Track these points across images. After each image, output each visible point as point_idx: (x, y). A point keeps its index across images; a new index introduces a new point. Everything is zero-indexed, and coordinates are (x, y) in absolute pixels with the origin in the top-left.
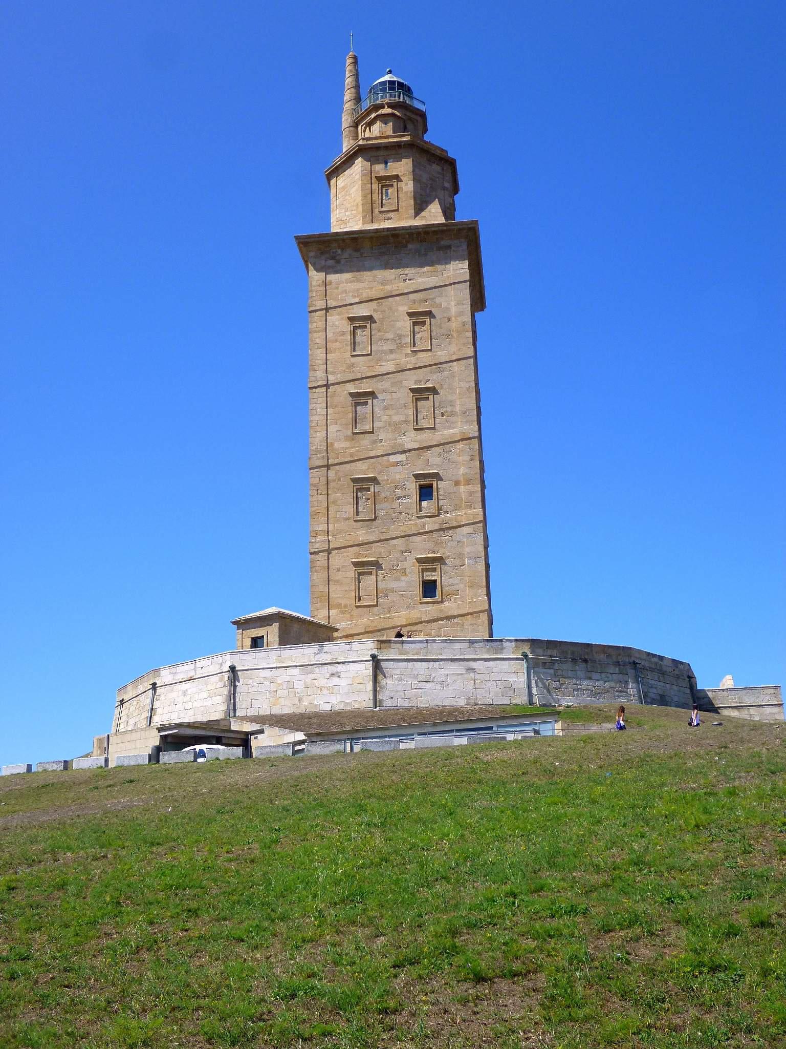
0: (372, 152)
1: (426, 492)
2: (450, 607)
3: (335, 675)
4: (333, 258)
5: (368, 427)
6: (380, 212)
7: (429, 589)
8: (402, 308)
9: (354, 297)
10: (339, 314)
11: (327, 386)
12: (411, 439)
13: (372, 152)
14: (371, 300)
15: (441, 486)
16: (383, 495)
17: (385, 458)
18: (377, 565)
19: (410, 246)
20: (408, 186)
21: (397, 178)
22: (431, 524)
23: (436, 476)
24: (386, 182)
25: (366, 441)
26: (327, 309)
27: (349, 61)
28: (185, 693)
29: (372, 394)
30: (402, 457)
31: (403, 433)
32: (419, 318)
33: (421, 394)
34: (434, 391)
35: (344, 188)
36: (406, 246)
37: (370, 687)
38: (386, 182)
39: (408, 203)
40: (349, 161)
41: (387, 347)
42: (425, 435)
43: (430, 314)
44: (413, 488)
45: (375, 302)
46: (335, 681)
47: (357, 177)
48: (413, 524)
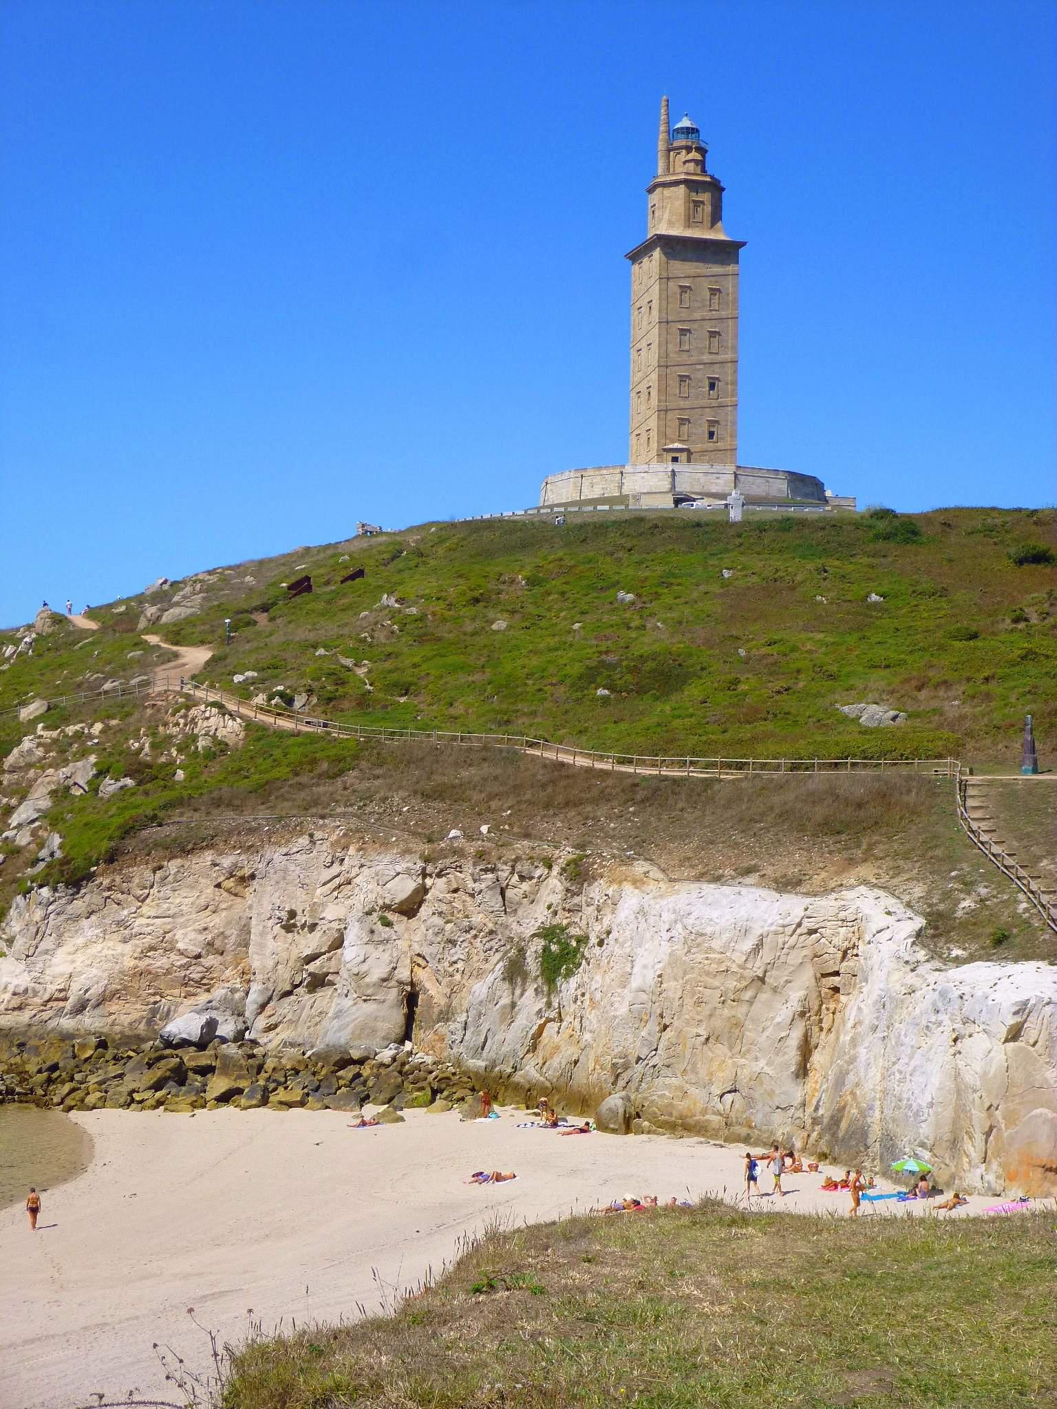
0: (691, 185)
1: (712, 386)
2: (720, 445)
5: (686, 348)
7: (711, 435)
8: (706, 284)
11: (667, 322)
12: (706, 358)
13: (691, 185)
15: (719, 385)
18: (688, 420)
20: (708, 209)
21: (702, 202)
22: (714, 403)
23: (717, 379)
24: (697, 204)
25: (685, 355)
26: (668, 279)
27: (664, 103)
29: (689, 331)
31: (703, 354)
32: (714, 292)
33: (713, 334)
34: (719, 333)
35: (670, 198)
38: (697, 204)
39: (707, 219)
40: (676, 183)
41: (697, 304)
43: (719, 290)
44: (707, 383)
48: (705, 402)
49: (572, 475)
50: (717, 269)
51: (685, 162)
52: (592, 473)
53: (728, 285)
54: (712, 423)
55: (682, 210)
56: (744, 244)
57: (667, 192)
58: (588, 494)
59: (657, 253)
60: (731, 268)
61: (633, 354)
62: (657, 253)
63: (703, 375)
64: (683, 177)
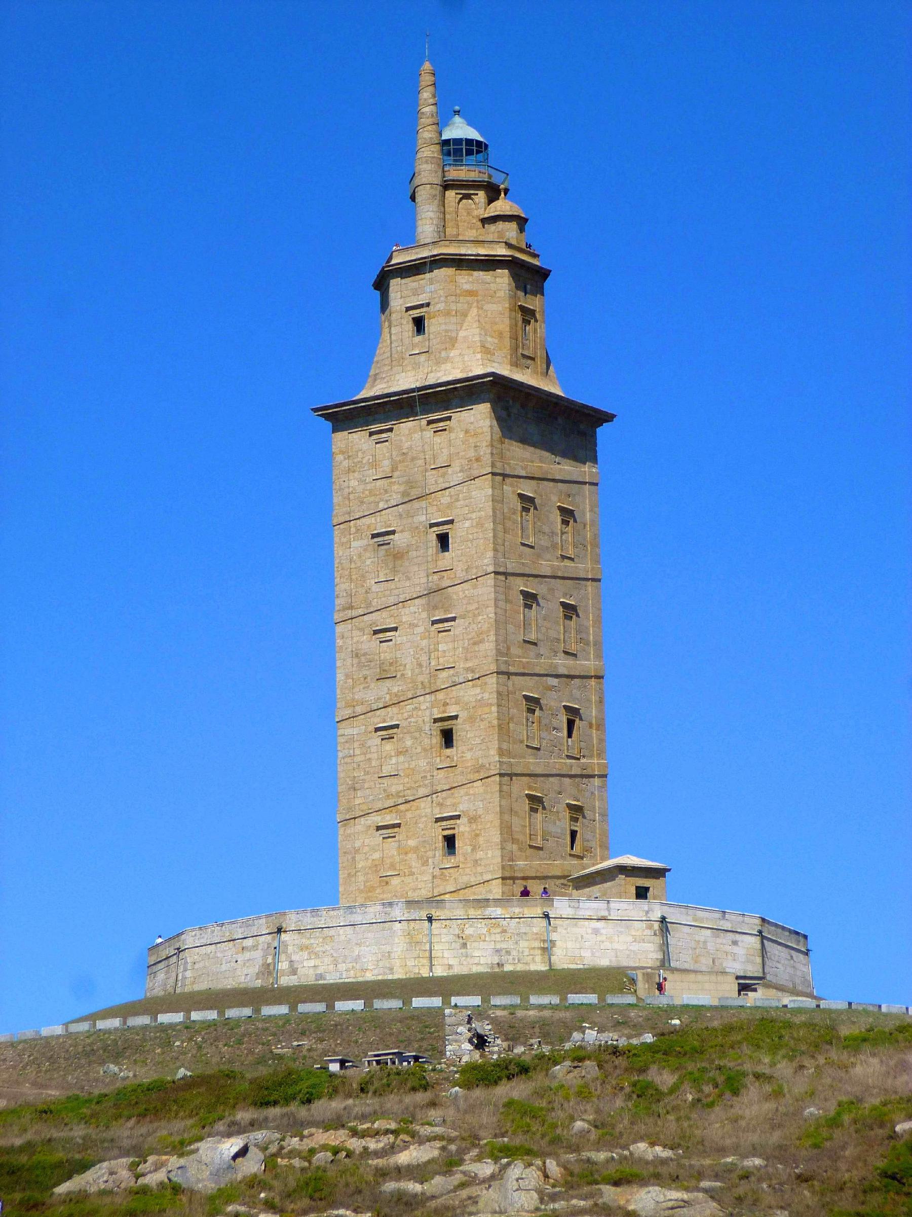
3: (735, 943)
4: (507, 409)
6: (524, 356)
9: (523, 468)
10: (512, 485)
12: (563, 664)
14: (532, 478)
16: (544, 722)
17: (545, 678)
19: (560, 420)
28: (596, 932)
30: (554, 682)
35: (471, 293)
36: (556, 419)
37: (759, 960)
40: (489, 264)
42: (570, 662)
45: (534, 482)
46: (736, 949)
47: (501, 294)
49: (398, 912)
50: (567, 468)
51: (485, 221)
52: (459, 912)
53: (585, 504)
54: (576, 811)
55: (504, 325)
56: (608, 418)
57: (467, 279)
58: (448, 961)
59: (478, 418)
60: (586, 471)
61: (350, 638)
62: (478, 418)
63: (556, 700)
64: (501, 251)
